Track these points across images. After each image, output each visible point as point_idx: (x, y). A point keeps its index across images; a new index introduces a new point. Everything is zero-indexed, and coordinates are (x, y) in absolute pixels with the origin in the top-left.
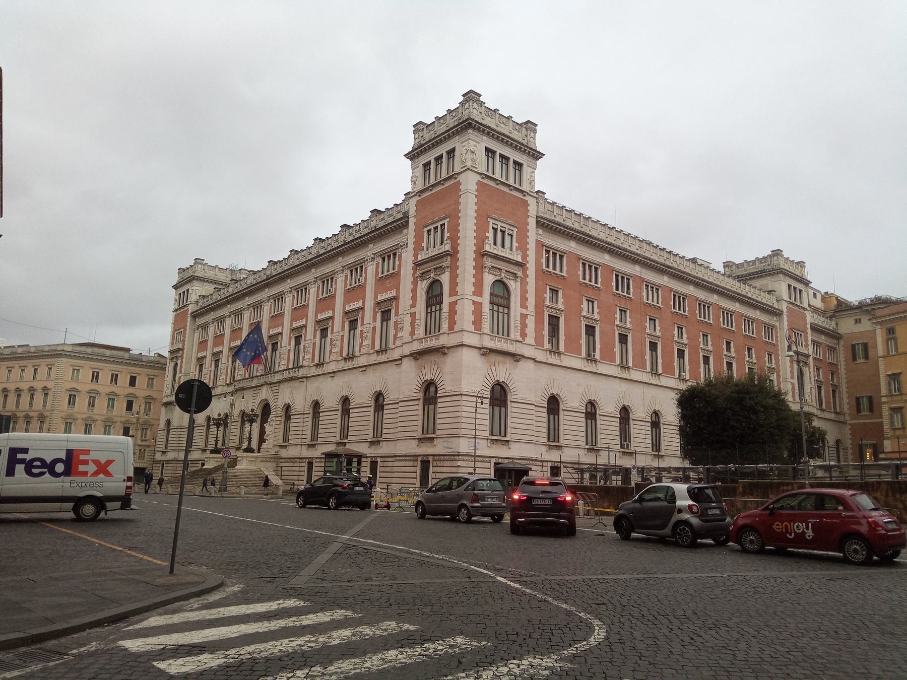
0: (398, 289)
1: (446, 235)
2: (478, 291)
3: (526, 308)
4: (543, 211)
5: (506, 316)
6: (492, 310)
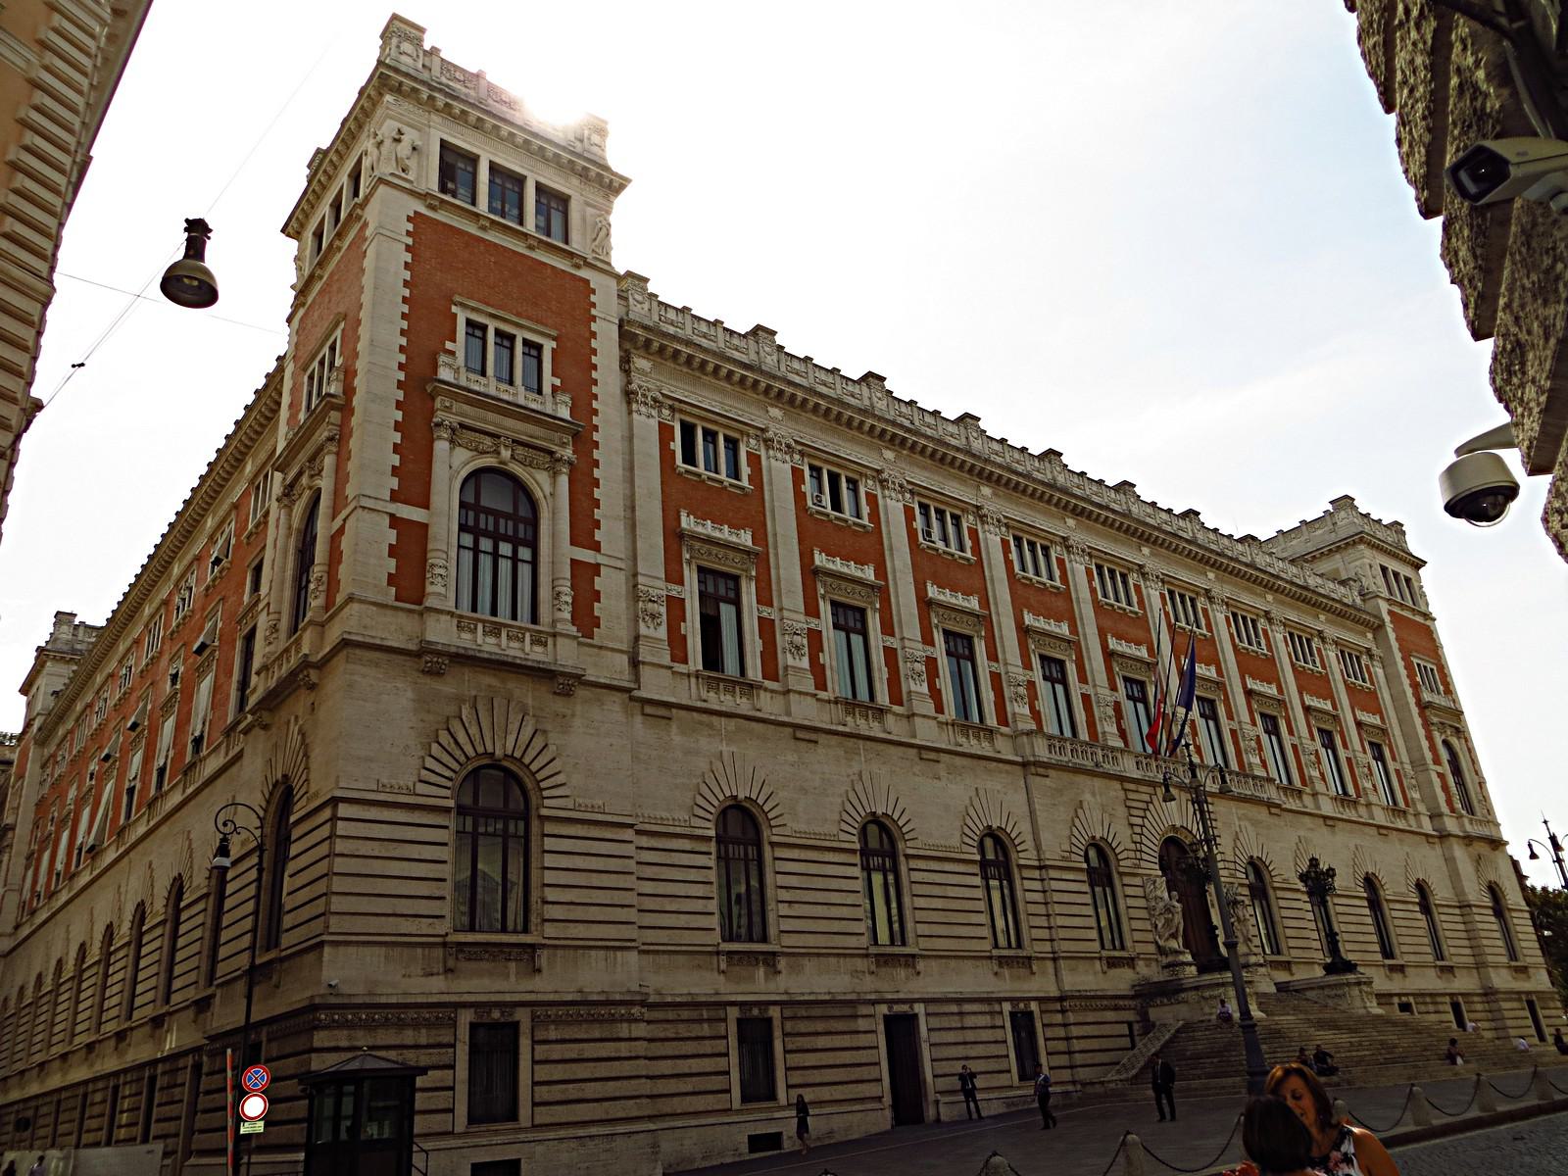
2: (413, 483)
3: (596, 547)
5: (525, 571)
6: (476, 551)
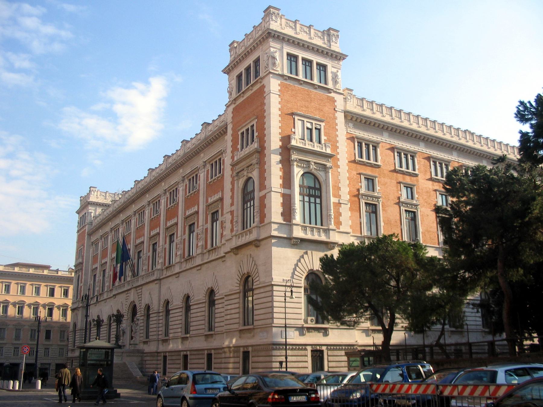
0: (223, 191)
1: (256, 134)
3: (340, 196)
4: (353, 107)
5: (318, 206)
